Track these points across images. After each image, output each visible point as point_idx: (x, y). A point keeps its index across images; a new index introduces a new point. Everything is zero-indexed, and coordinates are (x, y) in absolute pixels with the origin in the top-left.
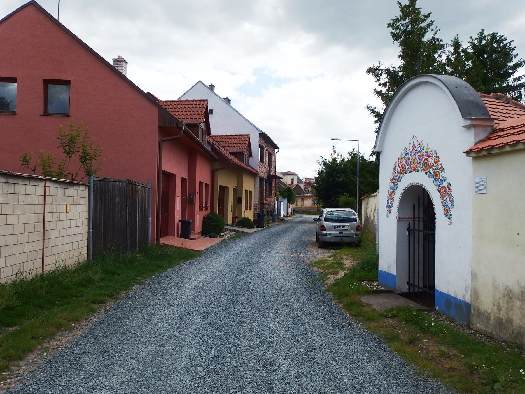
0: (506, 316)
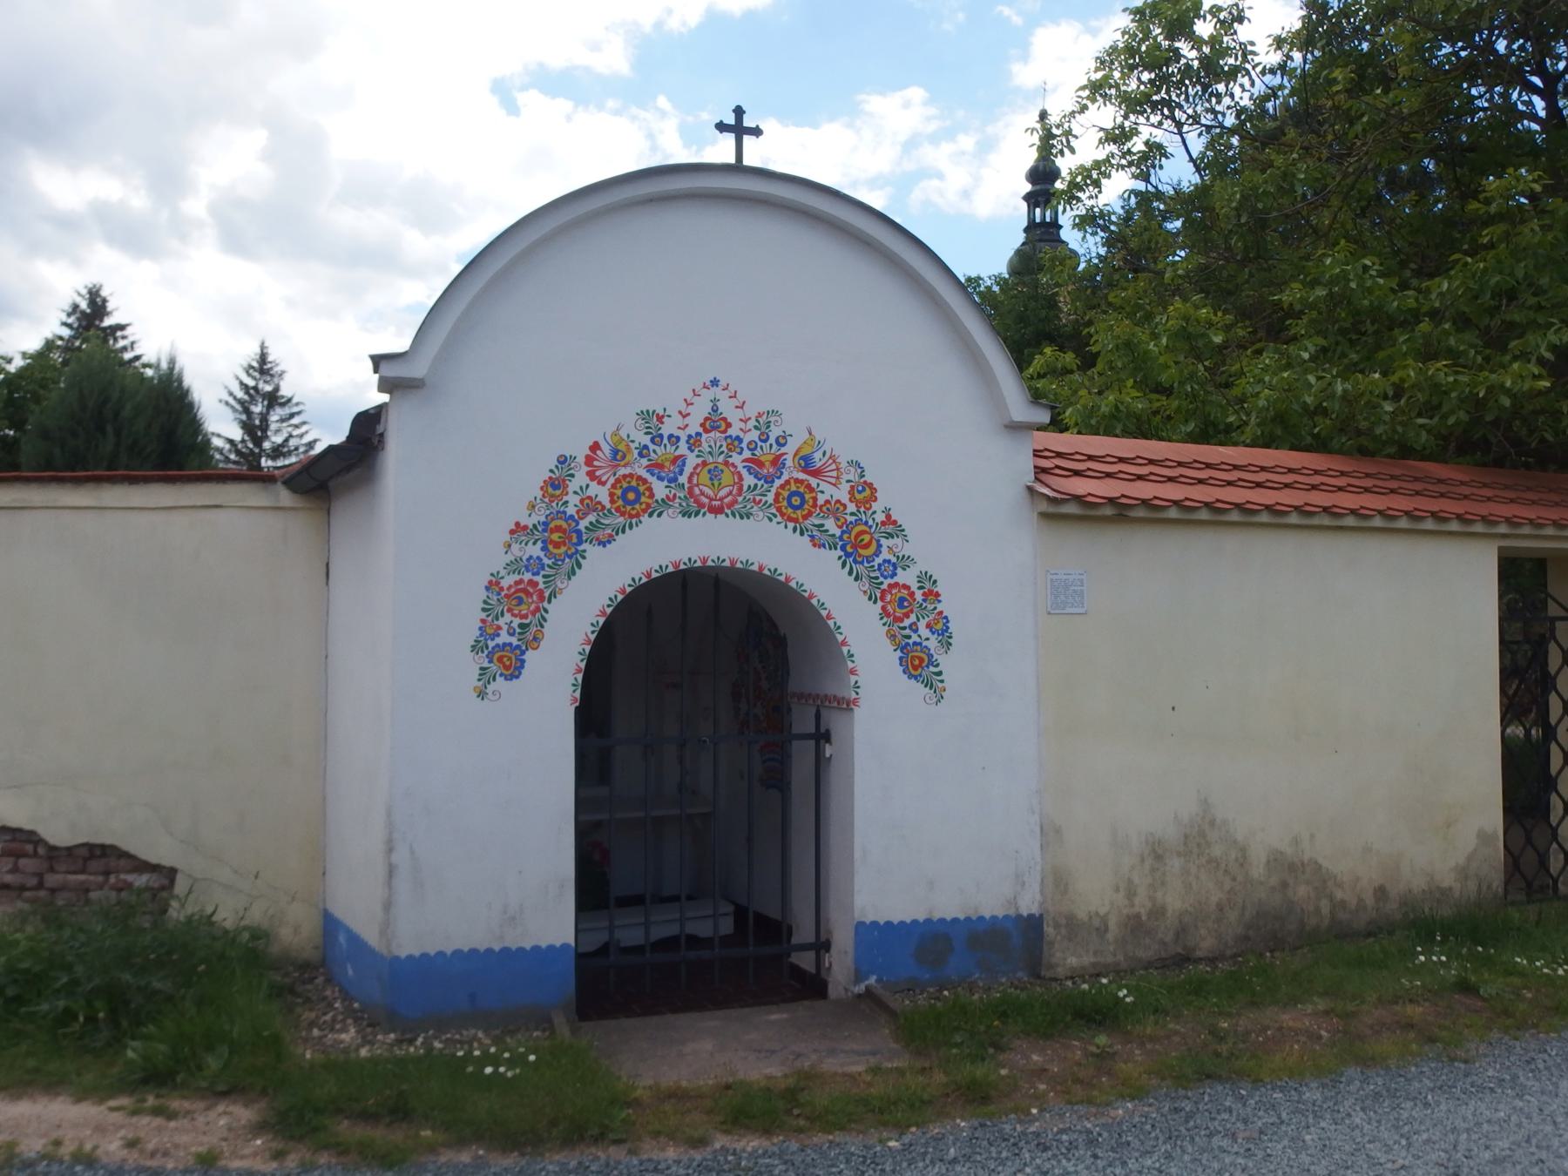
0: (1149, 905)
